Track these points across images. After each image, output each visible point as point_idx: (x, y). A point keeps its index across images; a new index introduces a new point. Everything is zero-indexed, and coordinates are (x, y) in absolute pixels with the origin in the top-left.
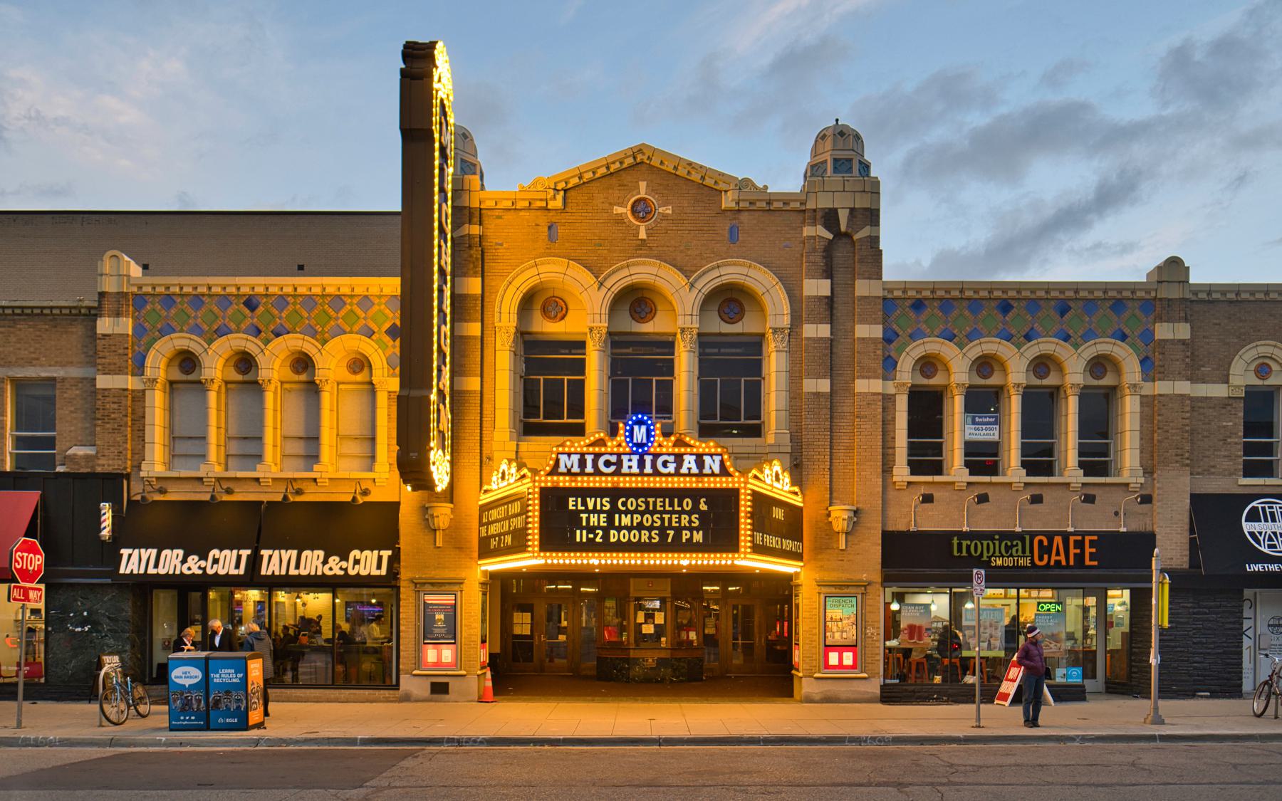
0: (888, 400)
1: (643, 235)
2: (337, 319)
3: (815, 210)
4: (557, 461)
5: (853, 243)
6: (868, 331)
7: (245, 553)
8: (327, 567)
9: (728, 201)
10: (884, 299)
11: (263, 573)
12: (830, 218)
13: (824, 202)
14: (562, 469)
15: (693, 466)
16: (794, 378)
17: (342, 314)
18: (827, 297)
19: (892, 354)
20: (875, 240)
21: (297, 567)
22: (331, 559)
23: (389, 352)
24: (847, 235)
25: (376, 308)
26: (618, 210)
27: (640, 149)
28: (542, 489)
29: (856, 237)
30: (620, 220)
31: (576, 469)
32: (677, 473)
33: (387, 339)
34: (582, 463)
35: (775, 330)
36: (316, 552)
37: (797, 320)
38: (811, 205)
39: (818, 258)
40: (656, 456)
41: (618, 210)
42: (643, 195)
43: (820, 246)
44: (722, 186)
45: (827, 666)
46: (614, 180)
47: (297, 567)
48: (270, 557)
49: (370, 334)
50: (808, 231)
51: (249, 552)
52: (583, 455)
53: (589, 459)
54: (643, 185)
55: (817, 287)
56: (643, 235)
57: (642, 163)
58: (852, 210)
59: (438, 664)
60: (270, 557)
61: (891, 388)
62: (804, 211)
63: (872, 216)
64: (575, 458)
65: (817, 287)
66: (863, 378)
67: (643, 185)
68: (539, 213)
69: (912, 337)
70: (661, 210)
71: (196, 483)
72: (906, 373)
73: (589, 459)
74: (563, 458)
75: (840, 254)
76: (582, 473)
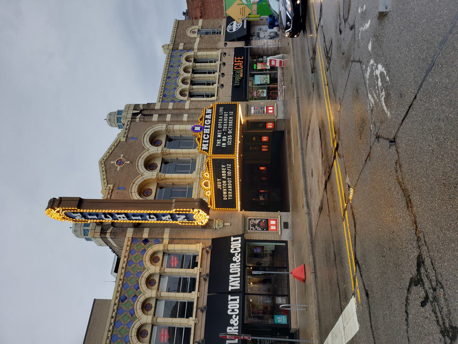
0: (191, 101)
1: (129, 162)
2: (136, 263)
3: (132, 118)
4: (204, 150)
5: (144, 110)
6: (171, 106)
7: (230, 297)
8: (237, 261)
9: (124, 140)
11: (239, 288)
12: (135, 115)
14: (207, 149)
15: (209, 115)
17: (134, 261)
20: (143, 105)
21: (237, 273)
22: (234, 260)
23: (153, 243)
25: (135, 248)
27: (101, 163)
28: (213, 159)
29: (142, 108)
30: (122, 169)
31: (207, 145)
32: (211, 119)
33: (148, 244)
34: (205, 143)
36: (231, 267)
37: (164, 122)
38: (130, 120)
39: (146, 118)
40: (205, 124)
42: (115, 162)
43: (143, 117)
45: (273, 112)
46: (108, 171)
47: (237, 273)
48: (232, 286)
49: (145, 250)
50: (137, 120)
51: (229, 296)
52: (202, 143)
53: (204, 141)
56: (129, 162)
58: (134, 109)
59: (276, 225)
60: (232, 286)
62: (131, 121)
63: (136, 107)
64: (203, 145)
65: (155, 118)
66: (184, 107)
68: (113, 192)
71: (200, 299)
73: (204, 141)
74: (203, 148)
75: (145, 112)
76: (209, 143)
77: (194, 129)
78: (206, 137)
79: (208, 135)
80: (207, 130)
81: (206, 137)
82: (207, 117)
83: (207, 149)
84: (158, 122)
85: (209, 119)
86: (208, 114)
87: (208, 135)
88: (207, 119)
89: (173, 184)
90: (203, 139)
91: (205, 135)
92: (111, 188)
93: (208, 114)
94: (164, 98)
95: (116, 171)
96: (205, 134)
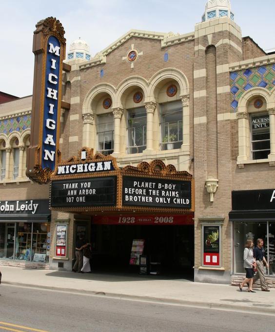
0: (234, 124)
9: (163, 44)
10: (230, 73)
13: (202, 33)
14: (59, 173)
16: (192, 116)
18: (204, 77)
19: (236, 99)
24: (213, 46)
26: (124, 58)
29: (216, 46)
30: (124, 63)
35: (185, 96)
38: (196, 37)
41: (124, 58)
44: (161, 38)
50: (196, 48)
54: (133, 46)
55: (200, 73)
56: (132, 66)
57: (132, 37)
61: (232, 116)
62: (194, 40)
66: (221, 113)
67: (133, 46)
69: (245, 88)
70: (139, 54)
72: (242, 107)
77: (84, 150)
78: (73, 169)
79: (75, 170)
80: (82, 168)
81: (73, 169)
82: (100, 165)
83: (59, 173)
84: (192, 81)
85: (95, 169)
86: (103, 165)
87: (75, 170)
88: (96, 165)
89: (97, 133)
90: (70, 166)
91: (75, 166)
92: (102, 62)
93: (103, 165)
94: (243, 71)
95: (122, 57)
96: (77, 167)
